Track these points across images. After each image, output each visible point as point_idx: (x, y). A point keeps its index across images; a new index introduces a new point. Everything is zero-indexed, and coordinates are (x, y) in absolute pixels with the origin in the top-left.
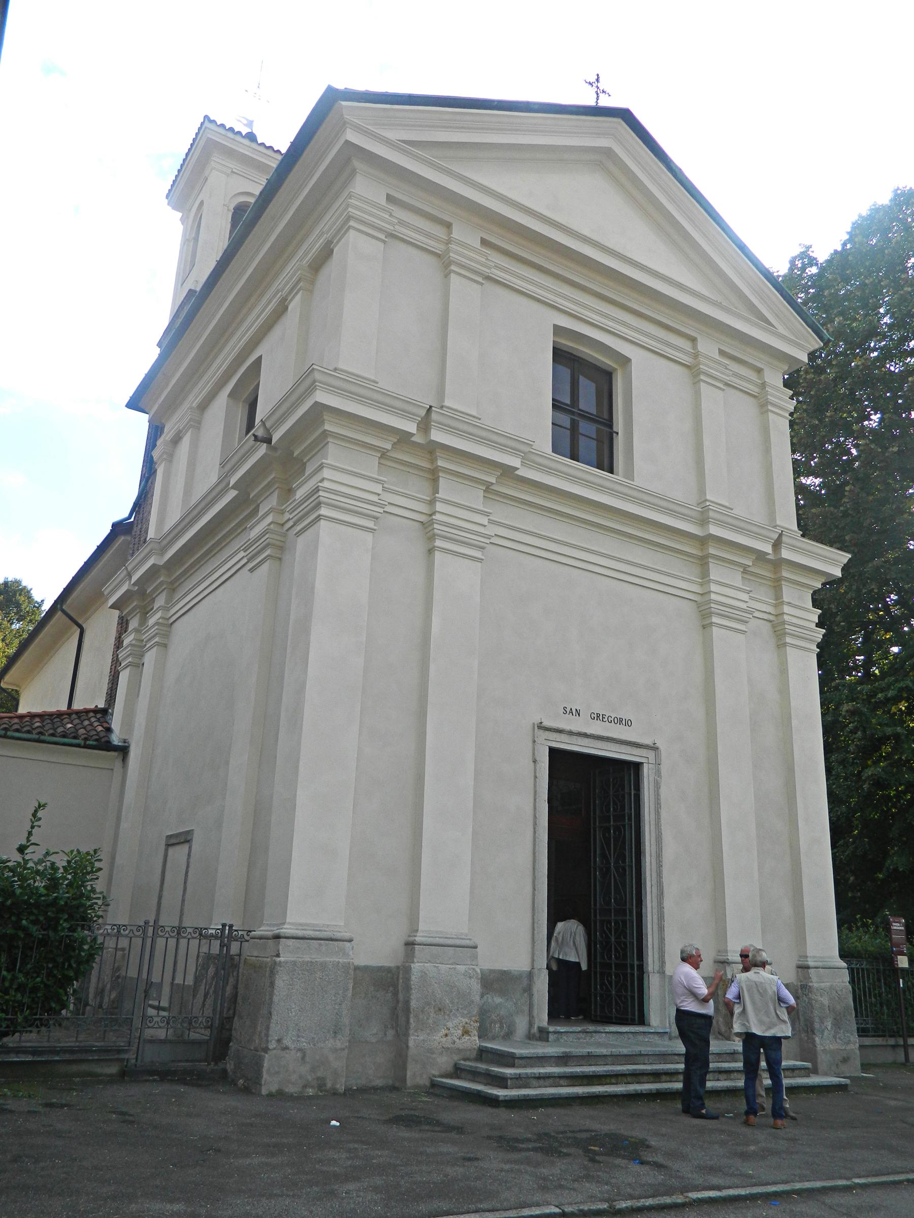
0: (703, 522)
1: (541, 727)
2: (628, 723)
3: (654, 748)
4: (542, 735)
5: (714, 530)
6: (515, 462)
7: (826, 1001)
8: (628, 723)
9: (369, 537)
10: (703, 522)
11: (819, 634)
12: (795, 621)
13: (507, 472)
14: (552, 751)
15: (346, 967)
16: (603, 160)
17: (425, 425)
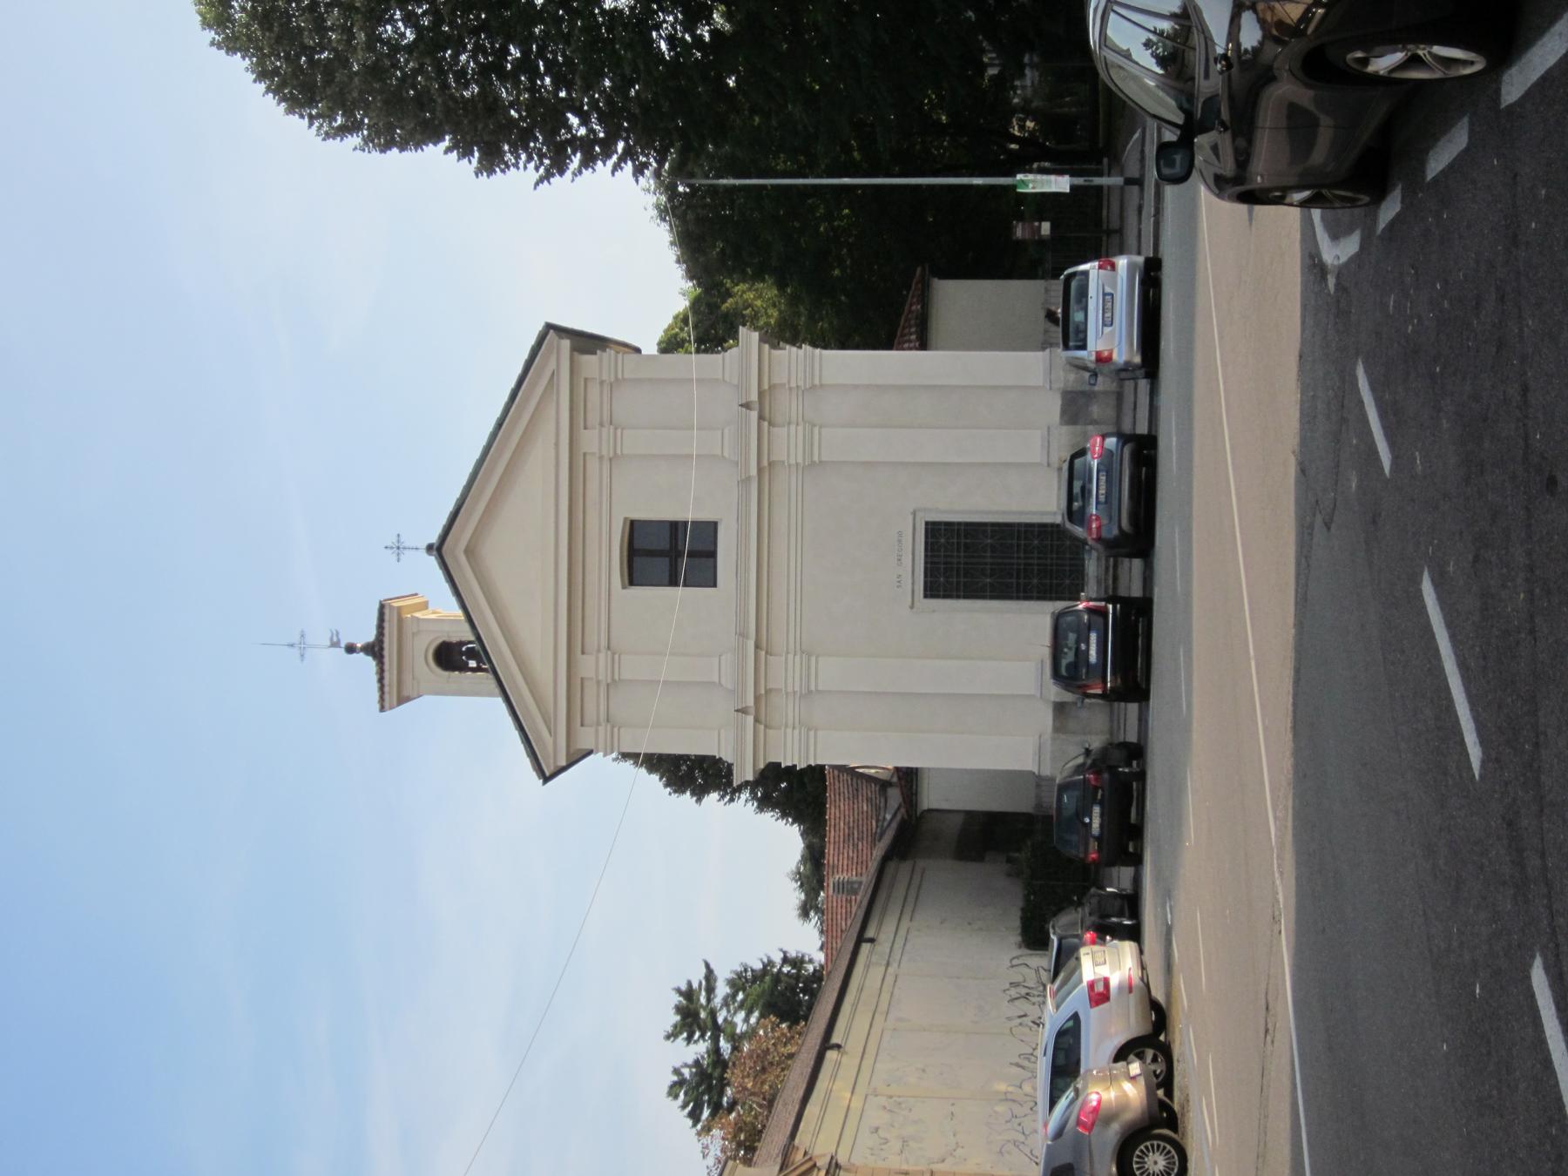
0: (749, 479)
1: (912, 607)
2: (900, 534)
3: (914, 514)
4: (917, 604)
5: (754, 472)
6: (751, 644)
7: (1072, 377)
8: (900, 534)
9: (820, 733)
10: (749, 479)
11: (807, 348)
12: (801, 375)
13: (757, 646)
14: (926, 596)
15: (1054, 739)
16: (470, 552)
17: (743, 711)
